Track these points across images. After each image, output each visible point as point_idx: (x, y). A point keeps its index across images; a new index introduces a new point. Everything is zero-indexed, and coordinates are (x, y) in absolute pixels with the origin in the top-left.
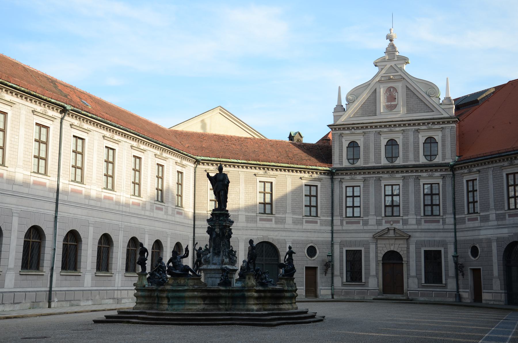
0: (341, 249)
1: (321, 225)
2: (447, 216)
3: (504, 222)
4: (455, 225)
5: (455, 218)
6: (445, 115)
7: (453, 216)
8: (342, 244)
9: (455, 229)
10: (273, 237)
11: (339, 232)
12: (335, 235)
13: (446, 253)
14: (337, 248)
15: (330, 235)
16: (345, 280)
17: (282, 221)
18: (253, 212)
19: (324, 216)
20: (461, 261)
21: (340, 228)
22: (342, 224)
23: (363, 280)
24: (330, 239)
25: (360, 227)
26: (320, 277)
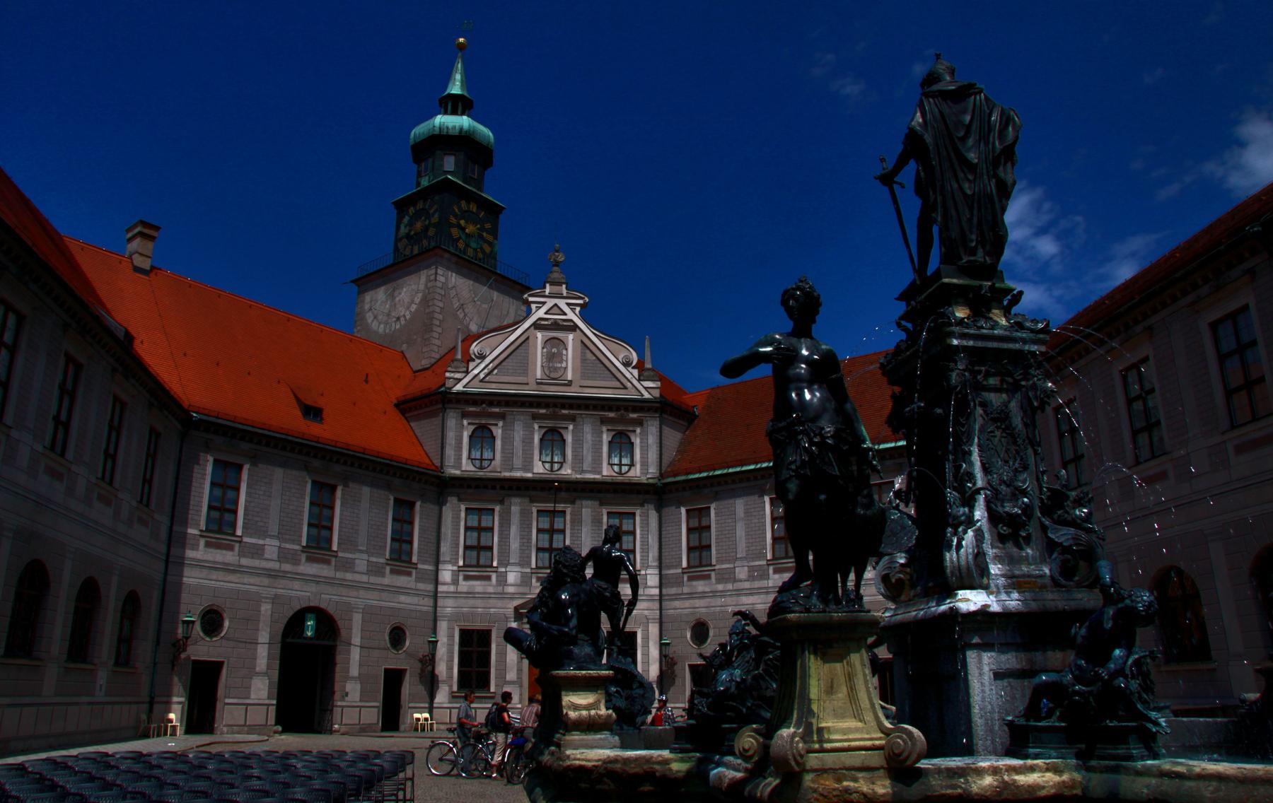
0: (451, 629)
1: (418, 580)
2: (649, 571)
3: (764, 583)
4: (660, 587)
5: (660, 574)
6: (647, 395)
7: (657, 571)
8: (453, 619)
9: (661, 594)
10: (327, 598)
11: (448, 595)
12: (440, 602)
13: (646, 639)
14: (443, 626)
15: (431, 602)
16: (455, 688)
17: (348, 566)
18: (293, 542)
19: (424, 562)
20: (670, 651)
21: (452, 588)
22: (455, 582)
23: (493, 689)
24: (431, 609)
25: (491, 587)
26: (409, 687)
